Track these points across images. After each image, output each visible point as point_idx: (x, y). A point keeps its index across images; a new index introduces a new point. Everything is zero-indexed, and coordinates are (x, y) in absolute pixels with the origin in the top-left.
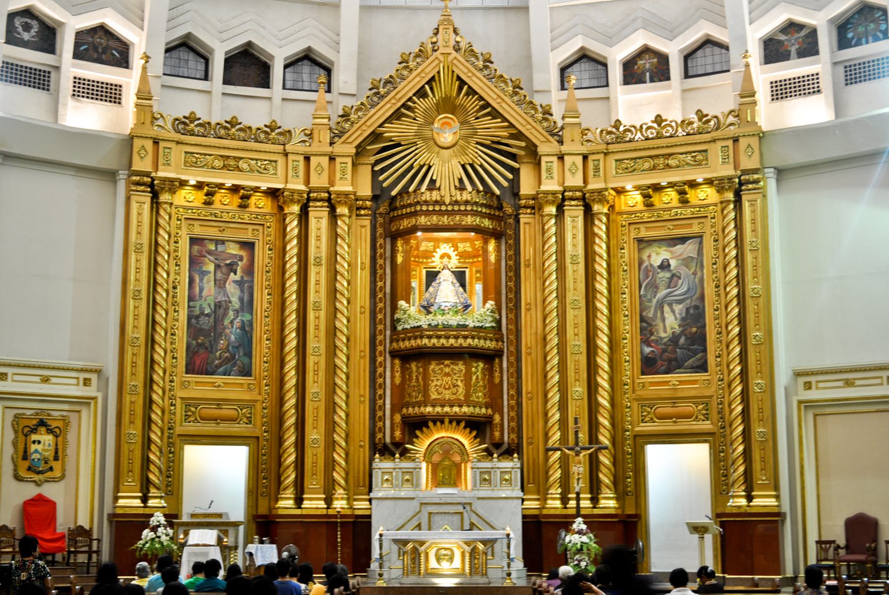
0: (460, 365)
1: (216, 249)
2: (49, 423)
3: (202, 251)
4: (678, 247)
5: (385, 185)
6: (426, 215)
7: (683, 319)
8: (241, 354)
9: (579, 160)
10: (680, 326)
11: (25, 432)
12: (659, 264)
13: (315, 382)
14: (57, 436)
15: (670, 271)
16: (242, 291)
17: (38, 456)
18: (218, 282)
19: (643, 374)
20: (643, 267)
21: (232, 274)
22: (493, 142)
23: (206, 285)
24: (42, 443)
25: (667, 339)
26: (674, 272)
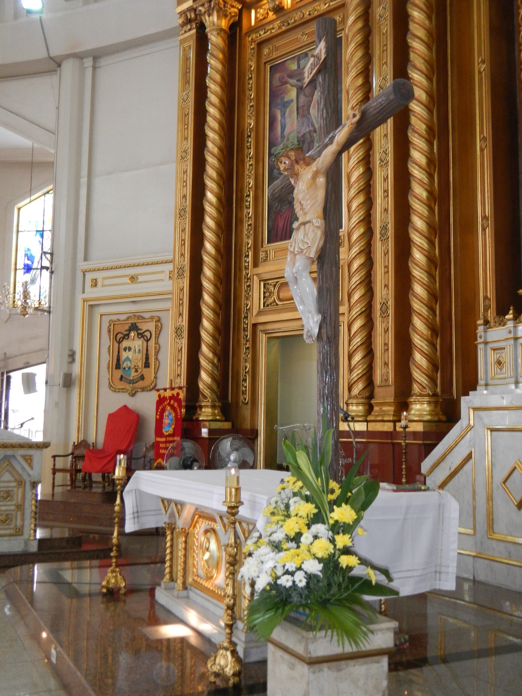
3: (283, 78)
11: (118, 340)
17: (129, 365)
18: (301, 111)
23: (288, 120)
24: (133, 350)
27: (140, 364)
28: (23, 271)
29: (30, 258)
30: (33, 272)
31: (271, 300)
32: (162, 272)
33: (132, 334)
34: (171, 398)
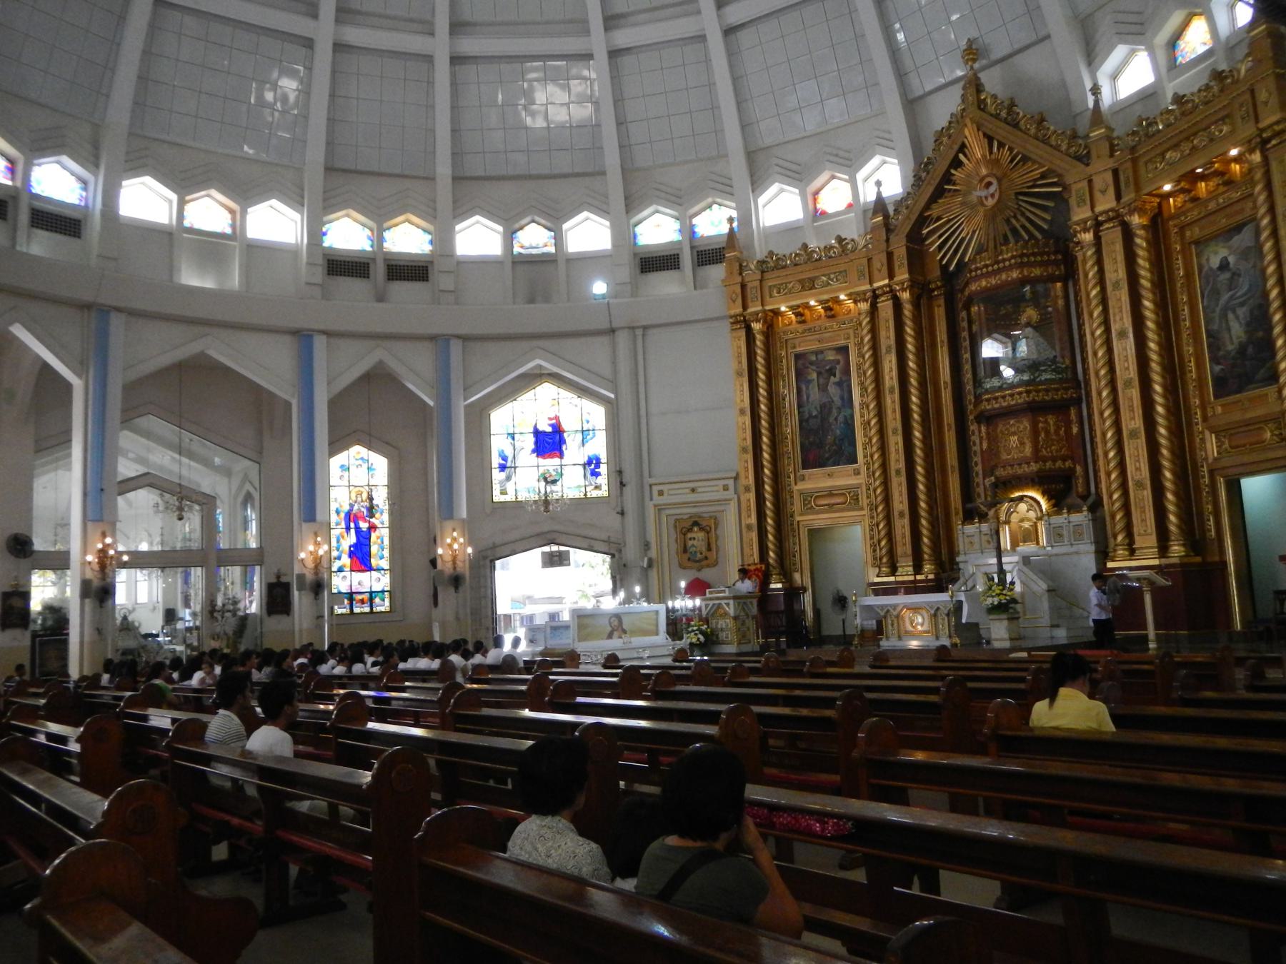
0: (1025, 423)
1: (817, 359)
2: (701, 523)
4: (1236, 238)
5: (944, 262)
6: (975, 281)
7: (1248, 324)
8: (846, 444)
9: (1109, 177)
10: (1246, 332)
12: (1217, 266)
13: (898, 461)
14: (708, 533)
15: (1229, 270)
16: (842, 390)
21: (832, 377)
22: (1029, 187)
23: (811, 392)
27: (704, 549)
28: (498, 470)
29: (505, 459)
30: (507, 470)
31: (809, 506)
32: (717, 486)
33: (696, 529)
34: (755, 570)
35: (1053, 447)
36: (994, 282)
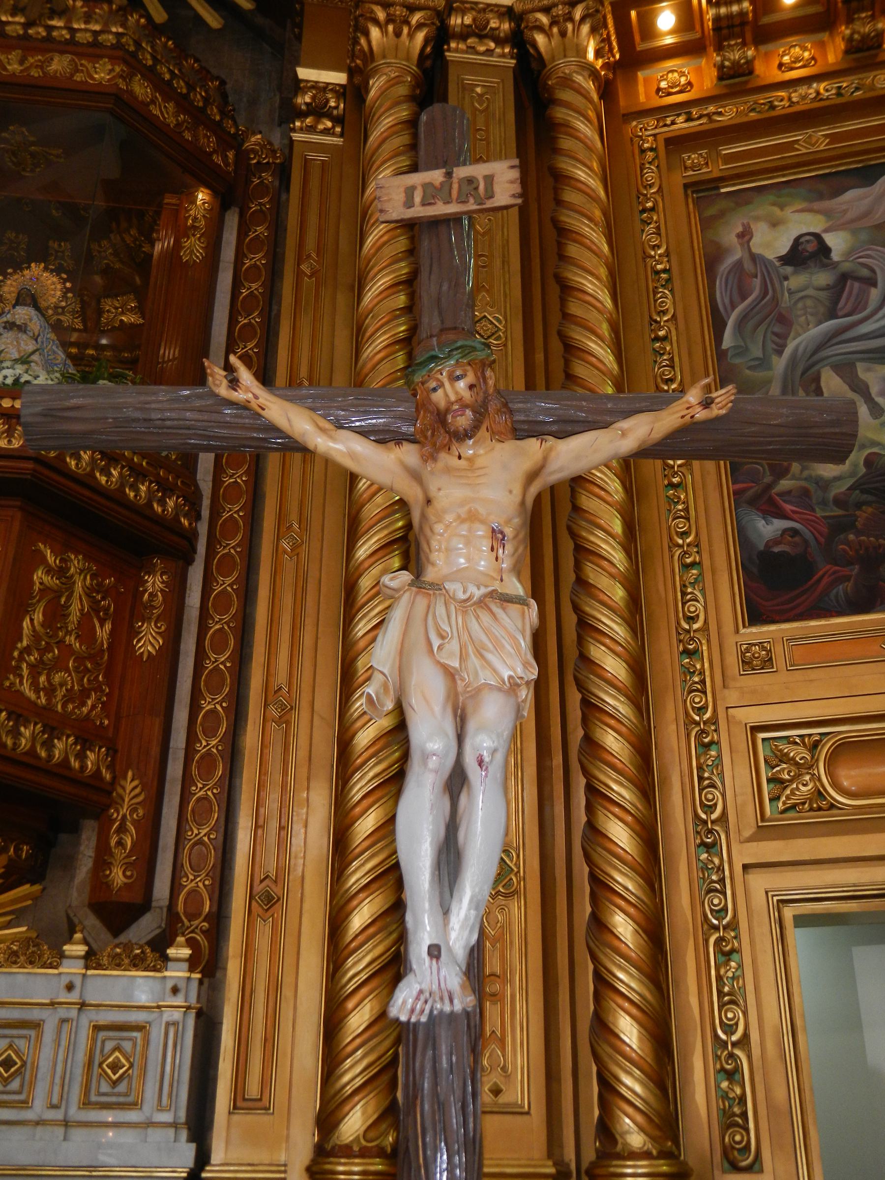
12: (783, 246)
19: (756, 616)
20: (724, 267)
25: (850, 482)
26: (846, 266)
35: (57, 678)
36: (14, 67)
